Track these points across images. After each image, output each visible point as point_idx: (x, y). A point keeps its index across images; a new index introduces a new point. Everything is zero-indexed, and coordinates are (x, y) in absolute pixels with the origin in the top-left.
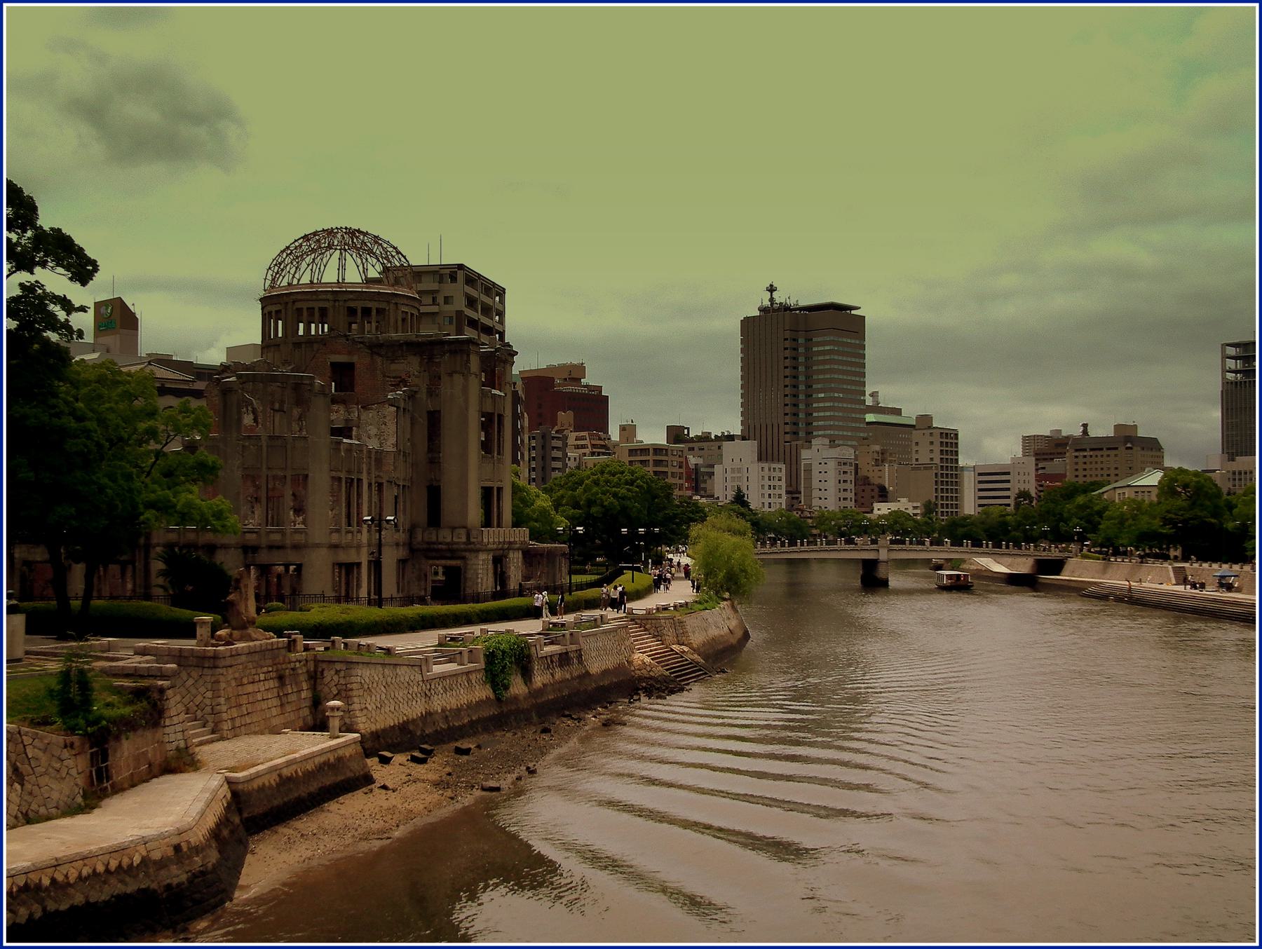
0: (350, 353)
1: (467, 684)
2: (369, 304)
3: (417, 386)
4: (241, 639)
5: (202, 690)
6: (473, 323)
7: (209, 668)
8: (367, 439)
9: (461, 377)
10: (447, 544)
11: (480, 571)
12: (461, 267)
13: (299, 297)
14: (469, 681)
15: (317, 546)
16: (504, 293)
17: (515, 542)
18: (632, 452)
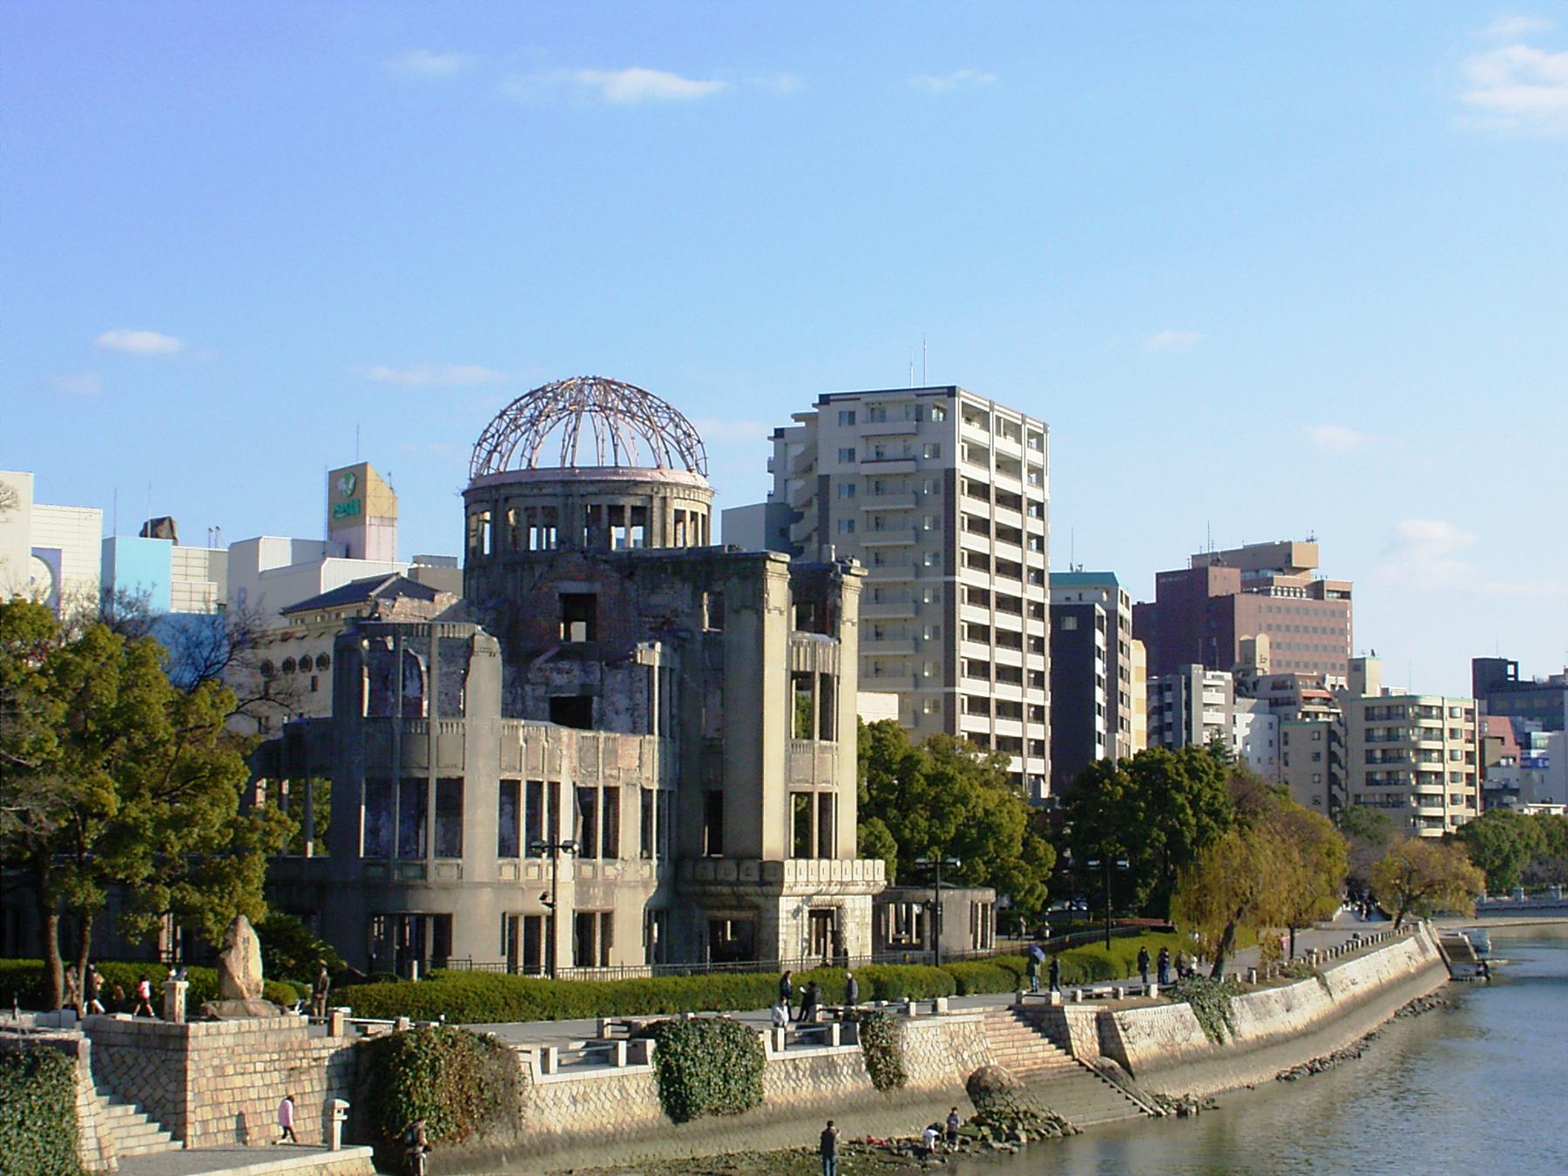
0: (590, 579)
1: (616, 1093)
2: (622, 501)
3: (687, 630)
4: (234, 1014)
5: (164, 1079)
6: (979, 490)
7: (174, 1050)
8: (614, 716)
9: (754, 617)
10: (731, 884)
11: (781, 930)
12: (951, 392)
13: (515, 491)
14: (622, 1089)
15: (482, 885)
16: (1046, 431)
17: (853, 883)
18: (1370, 711)
